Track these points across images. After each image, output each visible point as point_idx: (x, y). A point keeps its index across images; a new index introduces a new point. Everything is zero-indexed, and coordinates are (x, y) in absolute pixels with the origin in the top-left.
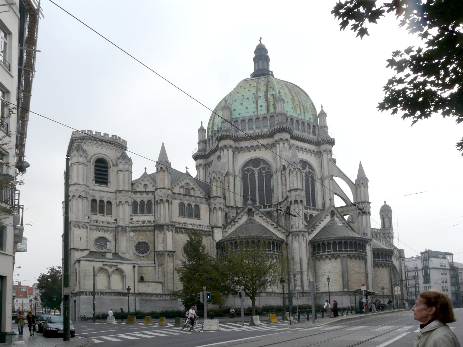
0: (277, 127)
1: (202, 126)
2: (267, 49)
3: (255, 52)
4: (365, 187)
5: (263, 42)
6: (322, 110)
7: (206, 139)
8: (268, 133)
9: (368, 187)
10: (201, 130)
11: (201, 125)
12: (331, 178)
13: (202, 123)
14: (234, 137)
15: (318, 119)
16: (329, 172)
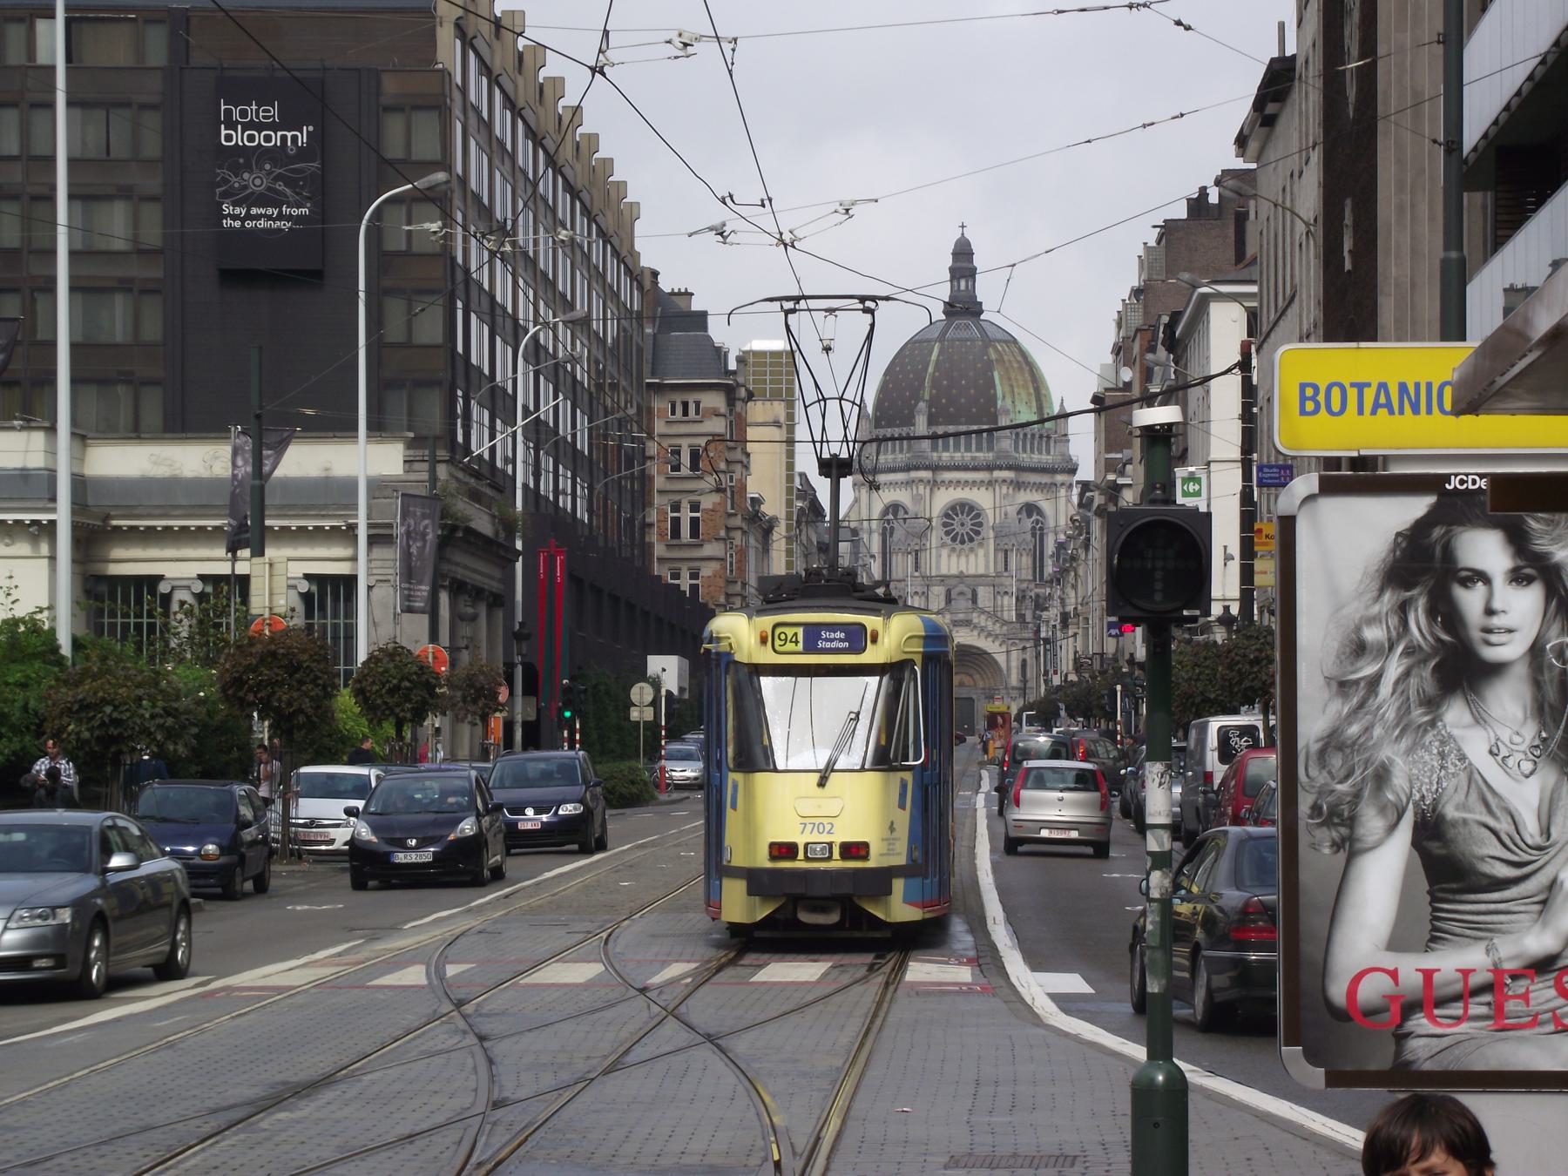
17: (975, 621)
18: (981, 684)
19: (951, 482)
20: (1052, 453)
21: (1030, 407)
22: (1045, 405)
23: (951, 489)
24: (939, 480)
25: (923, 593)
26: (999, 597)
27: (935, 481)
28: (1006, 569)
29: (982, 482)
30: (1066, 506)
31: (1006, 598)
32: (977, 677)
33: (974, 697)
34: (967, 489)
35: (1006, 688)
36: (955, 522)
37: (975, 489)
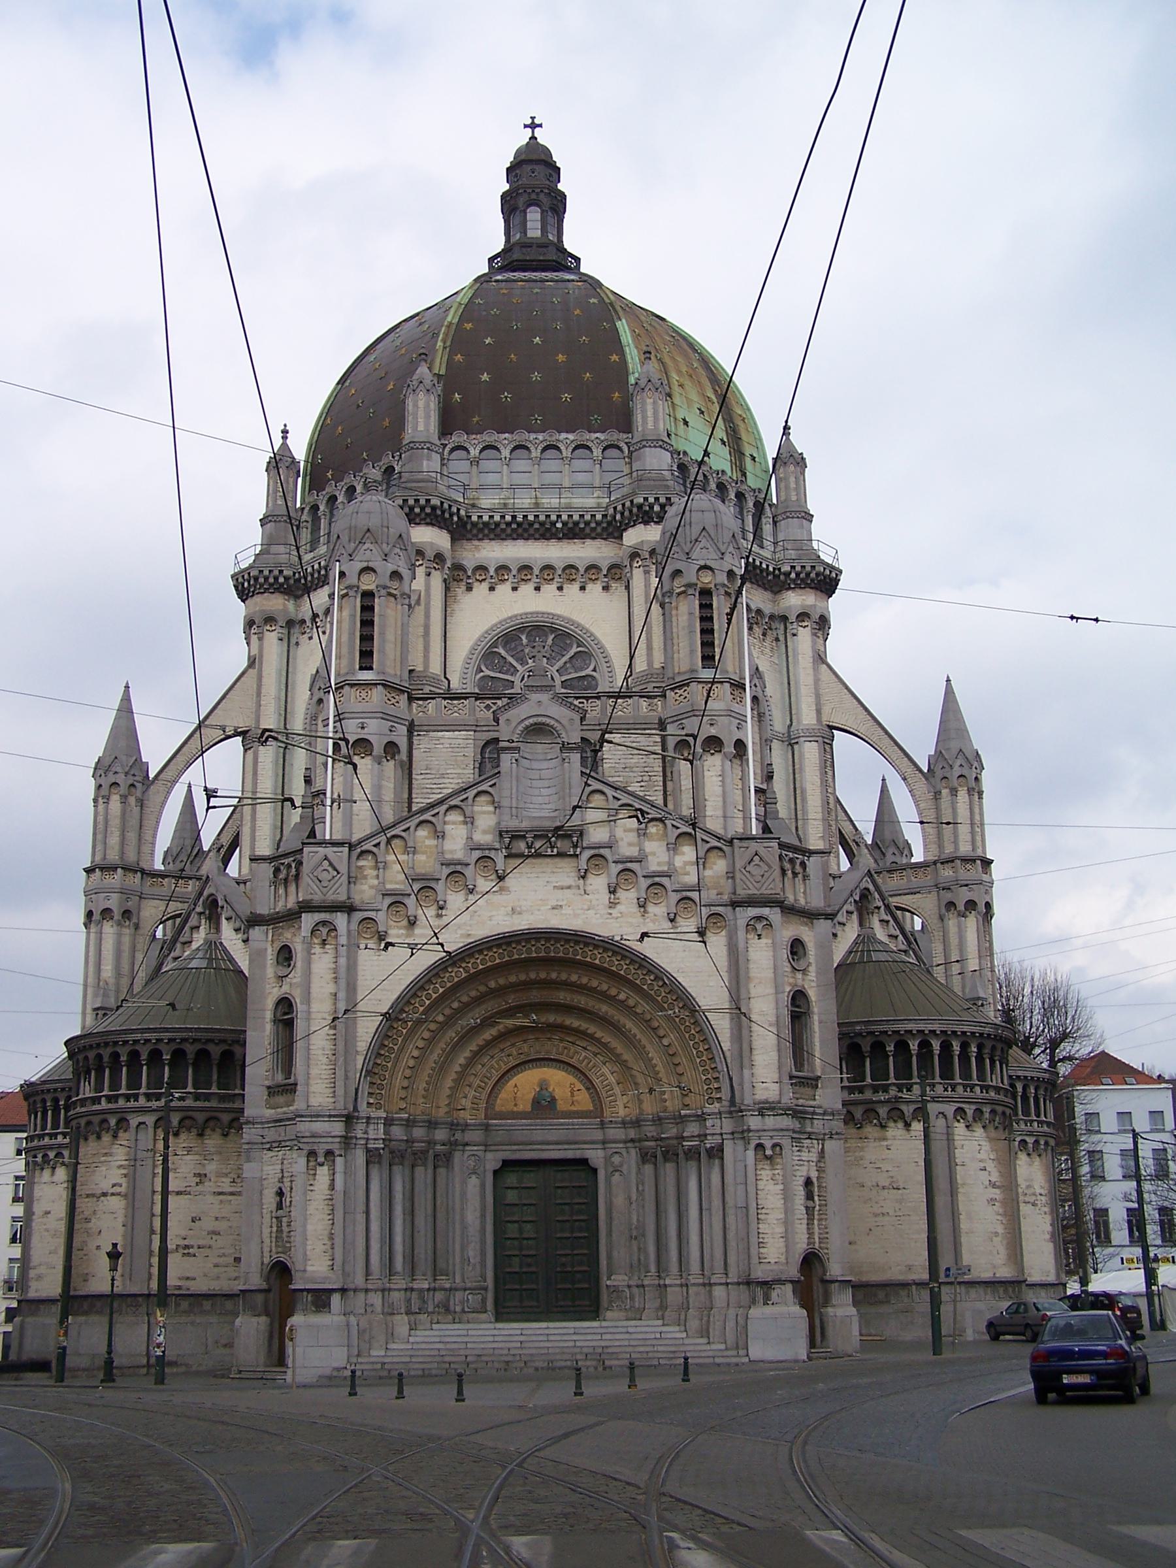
0: (646, 499)
1: (285, 446)
2: (558, 165)
3: (512, 171)
4: (970, 791)
5: (542, 137)
7: (298, 505)
8: (599, 517)
9: (980, 793)
10: (280, 463)
12: (826, 735)
14: (455, 518)
16: (819, 712)
17: (597, 835)
18: (621, 1107)
19: (503, 568)
22: (744, 436)
23: (504, 589)
24: (469, 565)
25: (391, 748)
27: (458, 567)
28: (708, 659)
29: (592, 567)
30: (816, 670)
31: (713, 765)
32: (606, 1075)
33: (595, 1156)
34: (549, 589)
35: (735, 1110)
36: (516, 679)
37: (572, 589)
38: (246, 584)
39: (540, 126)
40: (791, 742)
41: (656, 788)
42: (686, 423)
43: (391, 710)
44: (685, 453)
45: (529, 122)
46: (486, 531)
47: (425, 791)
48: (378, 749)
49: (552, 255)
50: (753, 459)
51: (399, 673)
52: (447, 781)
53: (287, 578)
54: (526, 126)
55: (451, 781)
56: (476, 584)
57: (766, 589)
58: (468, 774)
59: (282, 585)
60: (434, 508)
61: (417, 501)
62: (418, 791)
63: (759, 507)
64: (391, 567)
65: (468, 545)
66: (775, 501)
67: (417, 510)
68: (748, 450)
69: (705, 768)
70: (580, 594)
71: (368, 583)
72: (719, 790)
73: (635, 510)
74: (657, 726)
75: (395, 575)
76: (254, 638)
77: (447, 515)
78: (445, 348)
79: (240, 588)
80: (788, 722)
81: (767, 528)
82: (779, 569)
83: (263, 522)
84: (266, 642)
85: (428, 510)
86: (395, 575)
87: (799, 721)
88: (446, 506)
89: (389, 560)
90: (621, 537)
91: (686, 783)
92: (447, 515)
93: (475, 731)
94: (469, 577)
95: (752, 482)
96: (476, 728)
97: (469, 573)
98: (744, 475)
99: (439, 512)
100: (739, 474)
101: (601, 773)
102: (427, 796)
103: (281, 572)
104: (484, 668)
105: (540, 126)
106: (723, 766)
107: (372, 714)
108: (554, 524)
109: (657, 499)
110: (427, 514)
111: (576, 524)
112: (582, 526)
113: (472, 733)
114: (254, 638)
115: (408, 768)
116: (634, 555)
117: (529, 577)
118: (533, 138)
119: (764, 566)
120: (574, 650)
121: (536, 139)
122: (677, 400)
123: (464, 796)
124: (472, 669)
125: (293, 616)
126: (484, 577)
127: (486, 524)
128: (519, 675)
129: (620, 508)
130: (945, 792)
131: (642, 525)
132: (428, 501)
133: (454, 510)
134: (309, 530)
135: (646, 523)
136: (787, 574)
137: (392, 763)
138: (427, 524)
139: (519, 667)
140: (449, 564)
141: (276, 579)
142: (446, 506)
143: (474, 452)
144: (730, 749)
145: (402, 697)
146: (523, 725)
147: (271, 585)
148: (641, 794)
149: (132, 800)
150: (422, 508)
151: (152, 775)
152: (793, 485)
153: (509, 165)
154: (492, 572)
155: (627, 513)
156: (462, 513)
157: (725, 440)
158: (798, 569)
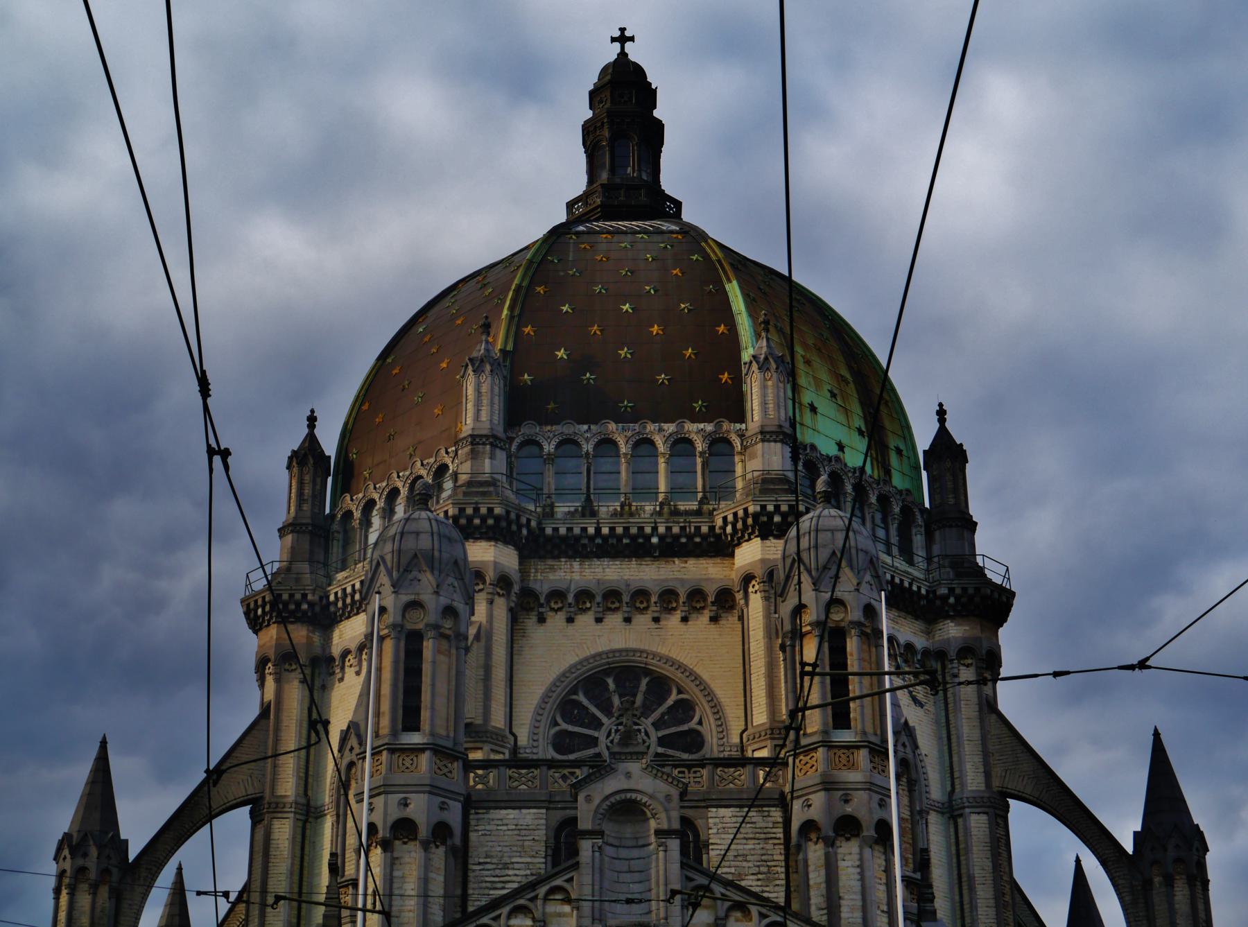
1: (311, 440)
5: (635, 53)
6: (943, 436)
7: (327, 511)
11: (306, 431)
13: (312, 420)
14: (525, 532)
15: (924, 474)
16: (988, 775)
19: (584, 595)
20: (920, 552)
21: (846, 411)
22: (887, 423)
25: (441, 832)
26: (815, 853)
31: (849, 853)
34: (642, 621)
36: (601, 735)
38: (260, 612)
39: (632, 39)
40: (952, 812)
41: (778, 882)
42: (813, 409)
43: (442, 782)
44: (813, 447)
45: (617, 34)
46: (563, 547)
47: (484, 885)
48: (423, 832)
49: (643, 199)
50: (899, 452)
51: (452, 735)
52: (511, 872)
53: (311, 605)
54: (613, 40)
55: (517, 872)
56: (551, 614)
57: (917, 618)
58: (540, 863)
59: (305, 612)
60: (497, 519)
61: (476, 510)
62: (476, 885)
63: (907, 512)
64: (443, 601)
65: (541, 566)
66: (927, 505)
67: (477, 521)
68: (893, 442)
69: (839, 857)
70: (682, 626)
71: (418, 621)
72: (857, 885)
73: (750, 521)
74: (776, 803)
75: (449, 611)
76: (270, 682)
77: (514, 528)
78: (511, 317)
79: (252, 615)
80: (949, 788)
81: (918, 540)
82: (934, 592)
83: (282, 532)
84: (286, 687)
85: (490, 522)
86: (449, 611)
87: (963, 785)
88: (513, 516)
89: (441, 593)
90: (732, 555)
91: (816, 877)
92: (514, 528)
93: (547, 809)
94: (541, 605)
95: (898, 481)
96: (549, 803)
97: (542, 601)
98: (888, 472)
99: (504, 524)
100: (882, 474)
101: (705, 865)
102: (486, 891)
103: (304, 596)
104: (559, 720)
105: (632, 39)
106: (861, 854)
107: (417, 788)
108: (648, 538)
109: (777, 507)
110: (489, 527)
111: (677, 537)
112: (683, 540)
113: (544, 811)
114: (270, 682)
115: (461, 857)
116: (747, 579)
117: (617, 605)
118: (623, 54)
119: (915, 588)
120: (674, 697)
121: (626, 55)
122: (802, 381)
123: (532, 895)
124: (545, 720)
125: (318, 651)
126: (560, 605)
127: (564, 539)
128: (604, 731)
129: (730, 518)
130: (1157, 880)
131: (759, 539)
132: (490, 510)
133: (524, 520)
134: (341, 543)
135: (764, 537)
136: (944, 598)
137: (442, 850)
138: (489, 539)
139: (605, 720)
140: (516, 588)
141: (298, 604)
142: (513, 516)
143: (549, 447)
144: (869, 832)
145: (455, 764)
146: (608, 803)
147: (292, 613)
148: (757, 889)
149: (104, 892)
150: (484, 519)
151: (132, 856)
152: (950, 485)
153: (592, 87)
154: (570, 599)
155: (740, 525)
156: (533, 524)
157: (864, 429)
158: (958, 591)
